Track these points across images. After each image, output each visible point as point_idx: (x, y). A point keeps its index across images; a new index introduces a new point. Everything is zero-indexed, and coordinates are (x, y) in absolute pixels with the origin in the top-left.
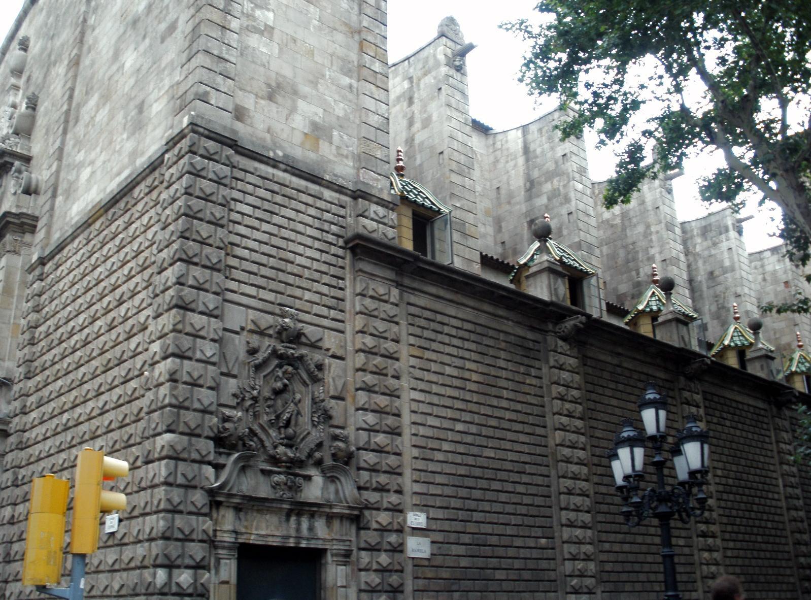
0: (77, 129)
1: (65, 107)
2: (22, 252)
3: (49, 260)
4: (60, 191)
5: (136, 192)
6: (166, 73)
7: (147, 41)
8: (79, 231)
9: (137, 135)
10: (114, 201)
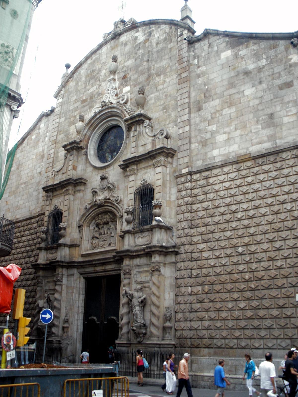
0: (202, 113)
1: (187, 100)
2: (168, 166)
4: (193, 140)
5: (284, 155)
7: (264, 86)
8: (227, 164)
9: (272, 128)
10: (262, 156)
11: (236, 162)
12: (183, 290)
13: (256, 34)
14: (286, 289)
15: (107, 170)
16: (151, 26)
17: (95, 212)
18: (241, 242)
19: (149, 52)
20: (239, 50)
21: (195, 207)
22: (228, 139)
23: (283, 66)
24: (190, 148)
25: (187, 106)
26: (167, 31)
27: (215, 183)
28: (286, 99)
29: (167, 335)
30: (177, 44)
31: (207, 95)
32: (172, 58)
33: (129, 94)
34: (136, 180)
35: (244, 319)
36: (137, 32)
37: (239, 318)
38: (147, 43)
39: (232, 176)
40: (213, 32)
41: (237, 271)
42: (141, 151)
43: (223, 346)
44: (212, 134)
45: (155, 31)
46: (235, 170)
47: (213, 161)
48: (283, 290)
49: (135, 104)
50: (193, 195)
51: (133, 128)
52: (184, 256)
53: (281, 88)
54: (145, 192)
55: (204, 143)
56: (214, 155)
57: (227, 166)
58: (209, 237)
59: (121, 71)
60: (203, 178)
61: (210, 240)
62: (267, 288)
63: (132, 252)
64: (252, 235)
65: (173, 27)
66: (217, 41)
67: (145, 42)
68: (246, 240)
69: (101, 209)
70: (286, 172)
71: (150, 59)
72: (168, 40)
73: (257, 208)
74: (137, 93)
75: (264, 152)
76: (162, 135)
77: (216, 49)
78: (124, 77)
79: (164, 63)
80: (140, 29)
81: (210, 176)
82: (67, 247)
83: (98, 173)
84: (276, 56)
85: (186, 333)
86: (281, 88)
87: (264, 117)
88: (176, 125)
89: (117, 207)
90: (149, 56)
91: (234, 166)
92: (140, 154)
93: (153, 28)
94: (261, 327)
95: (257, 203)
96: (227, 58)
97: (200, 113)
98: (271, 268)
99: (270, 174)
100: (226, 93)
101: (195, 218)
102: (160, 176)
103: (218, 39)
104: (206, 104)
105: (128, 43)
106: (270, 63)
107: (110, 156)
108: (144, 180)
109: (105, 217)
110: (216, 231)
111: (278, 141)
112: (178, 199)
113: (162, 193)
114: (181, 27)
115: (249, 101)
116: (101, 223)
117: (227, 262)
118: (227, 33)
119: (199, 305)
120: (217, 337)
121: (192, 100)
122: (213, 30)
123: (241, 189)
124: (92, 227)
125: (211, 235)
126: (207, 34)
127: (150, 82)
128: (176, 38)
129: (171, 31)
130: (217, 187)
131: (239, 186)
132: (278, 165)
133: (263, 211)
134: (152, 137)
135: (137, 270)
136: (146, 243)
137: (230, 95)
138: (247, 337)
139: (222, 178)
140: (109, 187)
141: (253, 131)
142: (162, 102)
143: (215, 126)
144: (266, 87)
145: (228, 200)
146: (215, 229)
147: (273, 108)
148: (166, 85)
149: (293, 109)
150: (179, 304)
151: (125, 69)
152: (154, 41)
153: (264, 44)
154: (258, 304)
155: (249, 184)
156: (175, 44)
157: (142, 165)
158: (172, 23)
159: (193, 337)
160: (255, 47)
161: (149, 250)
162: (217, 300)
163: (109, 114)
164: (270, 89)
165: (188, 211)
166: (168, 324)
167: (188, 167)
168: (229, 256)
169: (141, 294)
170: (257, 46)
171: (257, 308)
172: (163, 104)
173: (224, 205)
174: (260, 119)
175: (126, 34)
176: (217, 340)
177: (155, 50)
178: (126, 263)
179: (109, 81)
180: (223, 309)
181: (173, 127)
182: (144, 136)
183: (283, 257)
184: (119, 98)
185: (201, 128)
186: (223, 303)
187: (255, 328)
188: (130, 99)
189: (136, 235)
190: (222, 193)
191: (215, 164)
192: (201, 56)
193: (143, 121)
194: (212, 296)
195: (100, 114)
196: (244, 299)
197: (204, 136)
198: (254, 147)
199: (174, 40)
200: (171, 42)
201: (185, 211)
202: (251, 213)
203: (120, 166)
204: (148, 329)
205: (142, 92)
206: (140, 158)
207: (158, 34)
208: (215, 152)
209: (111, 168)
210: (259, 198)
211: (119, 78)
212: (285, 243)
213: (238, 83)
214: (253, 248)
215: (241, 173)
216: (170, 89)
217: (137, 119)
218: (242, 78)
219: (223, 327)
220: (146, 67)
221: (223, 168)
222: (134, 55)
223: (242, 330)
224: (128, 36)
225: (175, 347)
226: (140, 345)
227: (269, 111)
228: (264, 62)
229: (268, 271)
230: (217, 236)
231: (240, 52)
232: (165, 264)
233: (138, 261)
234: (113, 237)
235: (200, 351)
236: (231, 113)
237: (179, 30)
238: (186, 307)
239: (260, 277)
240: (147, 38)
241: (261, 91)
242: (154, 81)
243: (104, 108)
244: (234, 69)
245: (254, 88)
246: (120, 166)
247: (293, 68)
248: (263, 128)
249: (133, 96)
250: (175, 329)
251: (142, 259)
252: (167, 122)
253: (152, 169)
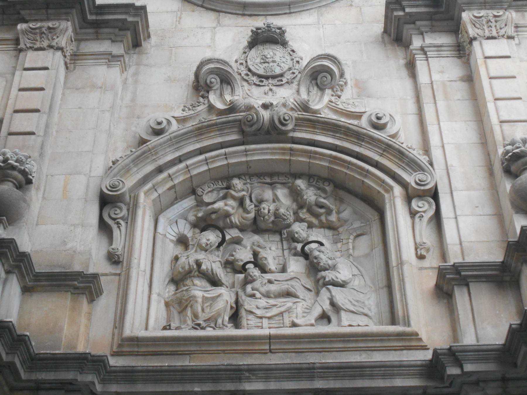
17: (219, 160)
69: (262, 153)
82: (22, 277)
109: (268, 194)
116: (235, 219)
124: (169, 230)
234: (342, 285)
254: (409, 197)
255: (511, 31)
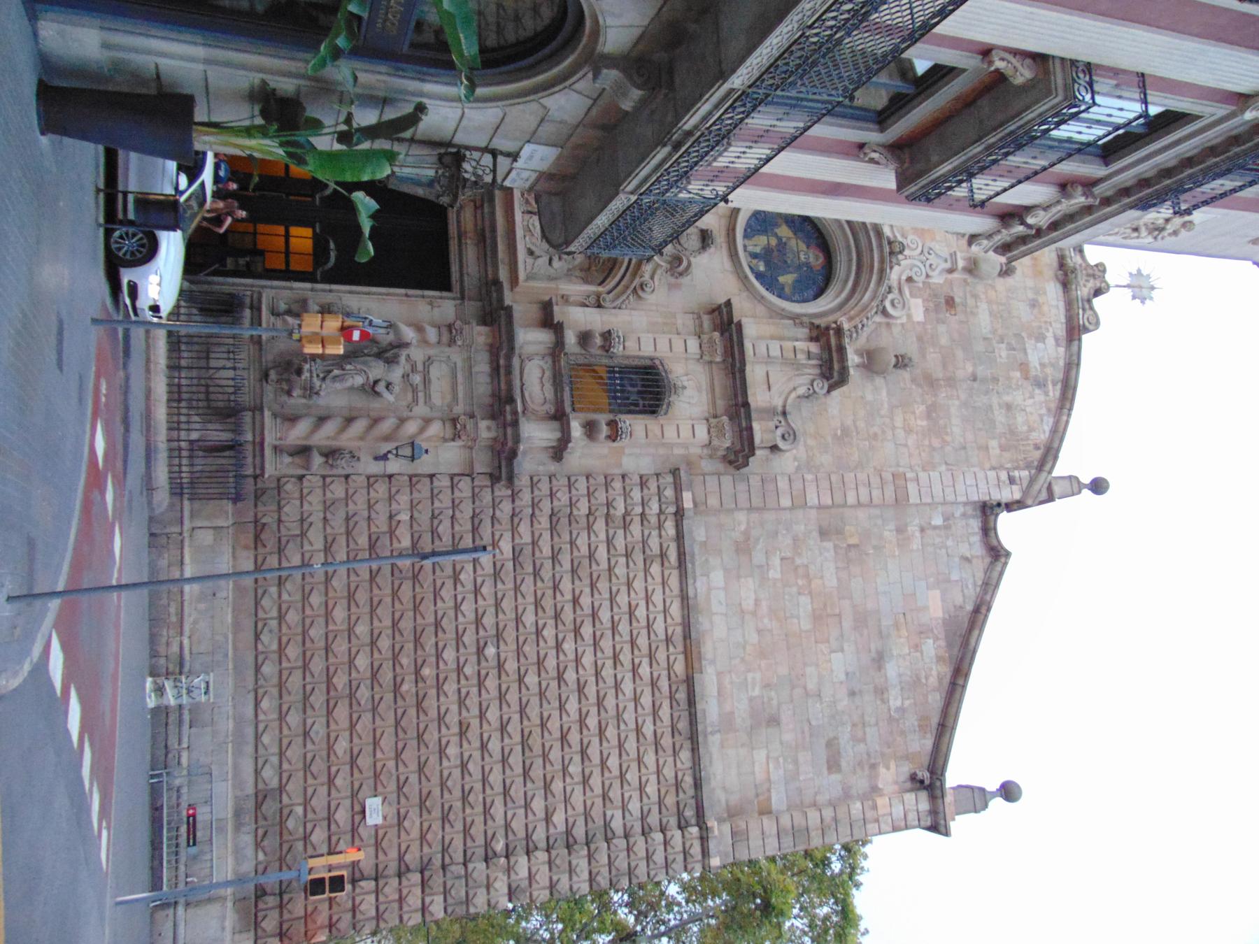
1: (851, 499)
3: (677, 526)
4: (755, 516)
5: (685, 755)
6: (790, 767)
7: (844, 703)
10: (691, 702)
11: (687, 636)
12: (404, 498)
13: (964, 687)
14: (394, 771)
15: (724, 246)
16: (1059, 386)
18: (509, 649)
19: (995, 380)
20: (936, 639)
21: (600, 526)
22: (742, 611)
23: (877, 748)
24: (737, 508)
25: (839, 499)
26: (1034, 435)
27: (649, 579)
28: (804, 757)
29: (288, 459)
30: (993, 468)
31: (851, 554)
32: (963, 452)
33: (904, 320)
34: (687, 359)
35: (328, 669)
36: (1057, 339)
37: (330, 655)
38: (1018, 374)
39: (659, 626)
40: (995, 574)
41: (441, 645)
42: (755, 373)
43: (261, 614)
44: (760, 567)
45: (1042, 398)
46: (670, 632)
47: (698, 573)
48: (391, 764)
49: (873, 345)
50: (628, 519)
51: (814, 348)
52: (487, 497)
53: (831, 744)
54: (652, 380)
55: (743, 548)
56: (712, 575)
57: (683, 609)
58: (525, 566)
59: (968, 288)
60: (665, 546)
61: (518, 567)
62: (397, 723)
63: (509, 358)
64: (521, 680)
65: (1037, 455)
66: (971, 581)
67: (1024, 367)
68: (511, 666)
70: (650, 759)
71: (976, 385)
72: (1012, 438)
73: (581, 689)
74: (901, 351)
75: (699, 707)
76: (783, 437)
77: (955, 576)
78: (950, 302)
79: (957, 430)
80: (1062, 350)
81: (666, 564)
83: (721, 217)
84: (903, 733)
85: (291, 511)
86: (831, 744)
87: (775, 702)
88: (798, 469)
89: (627, 287)
90: (984, 380)
91: (679, 630)
92: (748, 368)
93: (1051, 394)
94: (309, 712)
95: (591, 690)
96: (925, 608)
97: (815, 534)
98: (444, 730)
99: (649, 720)
100: (846, 603)
101: (574, 524)
102: (685, 432)
103: (975, 584)
104: (832, 552)
105: (1036, 311)
106: (891, 719)
107: (758, 250)
108: (684, 388)
110: (539, 584)
111: (718, 736)
112: (623, 477)
113: (644, 441)
114: (1032, 480)
115: (817, 665)
117: (464, 616)
118: (983, 610)
119: (363, 541)
120: (285, 597)
121: (848, 512)
122: (1001, 574)
123: (627, 648)
125: (530, 570)
126: (997, 554)
127: (919, 385)
128: (1009, 466)
129: (1031, 448)
130: (638, 585)
131: (633, 643)
132: (666, 741)
133: (572, 706)
134: (784, 406)
135: (459, 364)
136: (526, 395)
137: (839, 615)
138: (284, 678)
139: (657, 598)
140: (680, 261)
141: (750, 676)
142: (861, 424)
143: (778, 576)
144: (839, 708)
145: (605, 615)
146: (543, 581)
147: (791, 726)
148: (900, 433)
149: (781, 772)
150: (369, 486)
151: (971, 302)
152: (1017, 397)
153: (936, 700)
154: (363, 703)
155: (634, 670)
156: (994, 463)
157: (720, 378)
158: (1050, 453)
159: (282, 529)
160: (933, 681)
161: (509, 417)
162: (376, 591)
163: (866, 260)
164: (833, 717)
165: (593, 508)
166: (317, 460)
167: (695, 504)
168: (478, 622)
169: (397, 389)
170: (936, 684)
171: (354, 701)
172: (856, 428)
173: (596, 604)
174: (773, 693)
175: (1062, 305)
176: (275, 596)
177: (995, 401)
178: (480, 334)
179: (953, 255)
180: (353, 609)
181: (795, 459)
182: (790, 379)
183: (466, 758)
184: (900, 290)
185: (780, 537)
186: (367, 609)
187: (306, 698)
188: (891, 321)
189: (549, 360)
190: (622, 599)
191: (690, 581)
192: (947, 538)
193: (828, 379)
194: (385, 580)
195: (872, 234)
196: (376, 665)
197: (759, 547)
198: (714, 678)
199: (1007, 455)
200: (1003, 448)
201: (593, 501)
202: (570, 676)
203: (728, 303)
204: (304, 401)
205: (902, 362)
206: (738, 375)
207: (1032, 409)
208: (717, 577)
209: (728, 264)
210: (602, 694)
211: (951, 283)
212: (496, 762)
213: (862, 635)
214: (491, 683)
215: (662, 647)
216: (889, 447)
217: (836, 366)
218: (873, 647)
219: (308, 612)
220: (960, 374)
221: (679, 599)
222: (1000, 332)
223: (300, 663)
224: (1054, 311)
225: (256, 477)
226: (258, 377)
227: (785, 716)
228: (895, 701)
229: (436, 723)
230: (528, 587)
231: (931, 641)
232: (471, 448)
233: (482, 367)
234: (550, 263)
235: (246, 547)
236: (798, 619)
237: (1025, 474)
238: (359, 504)
239: (425, 704)
240: (1033, 373)
241: (833, 696)
242: (918, 399)
243: (887, 249)
244: (897, 626)
245: (842, 677)
246: (728, 303)
247: (867, 772)
248: (751, 699)
249: (896, 330)
250: (303, 476)
251: (488, 380)
252: (811, 442)
253: (705, 408)
254: (598, 296)
255: (707, 358)
